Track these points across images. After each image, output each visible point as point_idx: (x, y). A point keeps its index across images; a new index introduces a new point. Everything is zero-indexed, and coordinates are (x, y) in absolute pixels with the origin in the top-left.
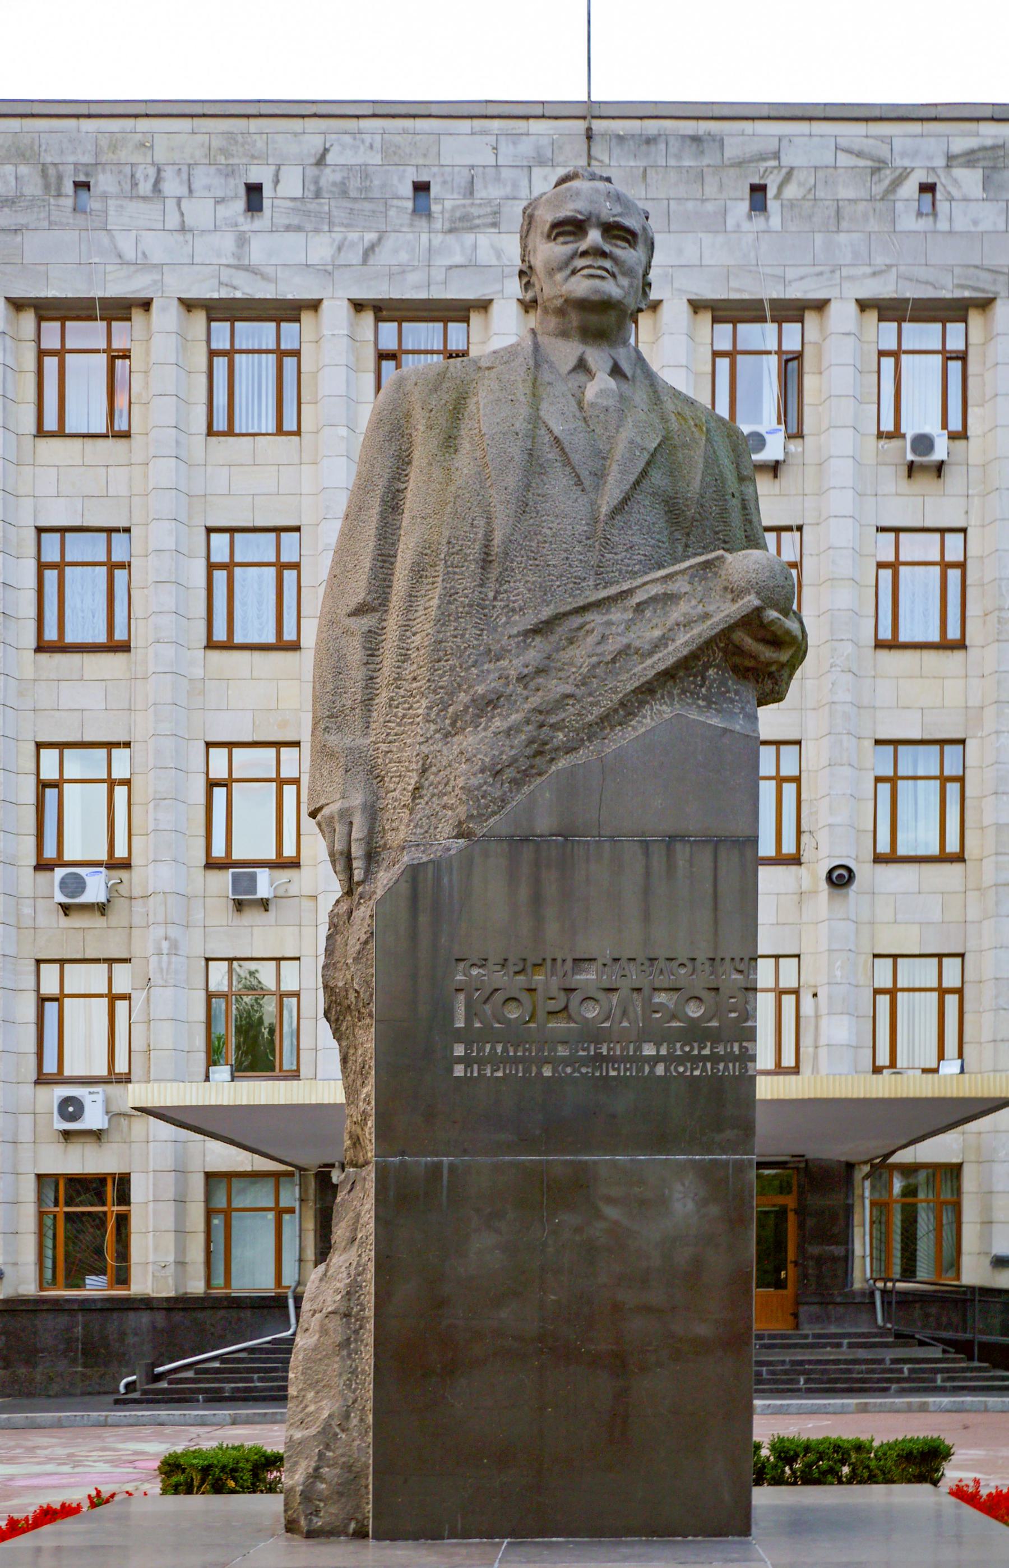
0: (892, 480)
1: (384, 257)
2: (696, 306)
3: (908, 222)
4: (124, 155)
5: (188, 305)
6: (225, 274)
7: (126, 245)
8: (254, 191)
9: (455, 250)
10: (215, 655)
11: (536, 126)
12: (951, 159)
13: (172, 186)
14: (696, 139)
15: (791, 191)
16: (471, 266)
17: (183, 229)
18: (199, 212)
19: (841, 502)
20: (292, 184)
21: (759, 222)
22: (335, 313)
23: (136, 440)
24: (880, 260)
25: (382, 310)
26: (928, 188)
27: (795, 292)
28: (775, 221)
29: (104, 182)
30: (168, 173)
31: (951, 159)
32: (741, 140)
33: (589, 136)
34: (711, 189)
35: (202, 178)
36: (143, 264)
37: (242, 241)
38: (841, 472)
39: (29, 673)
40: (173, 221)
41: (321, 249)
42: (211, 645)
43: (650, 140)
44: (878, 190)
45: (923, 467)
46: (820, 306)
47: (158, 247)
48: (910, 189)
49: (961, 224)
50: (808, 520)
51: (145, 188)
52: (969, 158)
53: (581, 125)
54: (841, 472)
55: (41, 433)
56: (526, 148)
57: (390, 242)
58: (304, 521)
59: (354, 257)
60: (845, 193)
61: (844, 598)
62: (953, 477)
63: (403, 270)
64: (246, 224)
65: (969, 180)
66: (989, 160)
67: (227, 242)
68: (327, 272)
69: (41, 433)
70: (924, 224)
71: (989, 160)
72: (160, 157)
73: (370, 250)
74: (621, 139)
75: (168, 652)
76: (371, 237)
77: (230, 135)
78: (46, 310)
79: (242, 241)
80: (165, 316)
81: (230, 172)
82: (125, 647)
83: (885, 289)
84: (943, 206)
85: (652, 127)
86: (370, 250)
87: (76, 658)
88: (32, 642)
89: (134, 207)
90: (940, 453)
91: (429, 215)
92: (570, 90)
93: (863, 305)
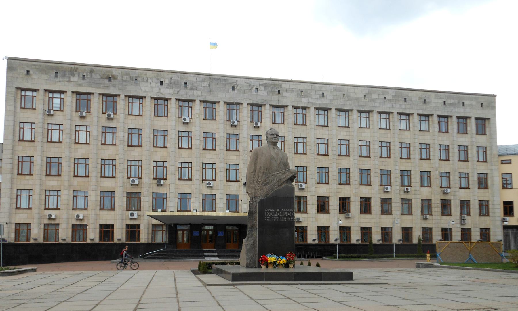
0: (252, 128)
1: (180, 93)
2: (225, 103)
3: (254, 93)
4: (143, 76)
5: (151, 98)
6: (157, 94)
7: (143, 88)
8: (161, 83)
9: (191, 93)
10: (155, 148)
11: (202, 76)
12: (260, 85)
13: (149, 81)
14: (225, 80)
15: (238, 88)
16: (193, 95)
17: (151, 87)
18: (153, 84)
19: (245, 131)
20: (167, 82)
21: (233, 92)
22: (173, 100)
23: (143, 116)
24: (250, 98)
25: (180, 100)
26: (257, 89)
27: (239, 102)
28: (236, 92)
29: (139, 79)
30: (149, 79)
31: (260, 85)
32: (231, 80)
33: (210, 78)
34: (227, 87)
35: (154, 80)
36: (145, 91)
37: (160, 89)
38: (245, 127)
39: (126, 149)
40: (149, 85)
41: (171, 91)
42: (154, 147)
43: (218, 79)
44: (250, 88)
45: (256, 127)
46: (242, 104)
47: (147, 89)
48: (254, 88)
49: (261, 94)
50: (240, 133)
51: (145, 80)
52: (262, 85)
53: (209, 77)
54: (245, 127)
55: (129, 115)
56: (201, 79)
57: (181, 91)
58: (168, 130)
59: (176, 93)
60: (246, 88)
61: (245, 144)
62: (260, 128)
63: (183, 95)
64: (160, 87)
65: (262, 88)
66: (265, 85)
67: (158, 89)
68: (172, 94)
69: (129, 115)
70: (256, 93)
71: (265, 85)
72: (148, 76)
73: (178, 92)
74: (214, 79)
75: (148, 147)
76: (178, 90)
77: (158, 74)
78: (130, 97)
79: (160, 89)
80: (148, 99)
81: (158, 79)
82: (141, 146)
83: (251, 102)
84: (259, 91)
85: (219, 77)
86: (178, 92)
87: (133, 148)
88: (127, 145)
89: (144, 83)
90: (259, 125)
91: (187, 87)
92: (207, 72)
93: (248, 104)
